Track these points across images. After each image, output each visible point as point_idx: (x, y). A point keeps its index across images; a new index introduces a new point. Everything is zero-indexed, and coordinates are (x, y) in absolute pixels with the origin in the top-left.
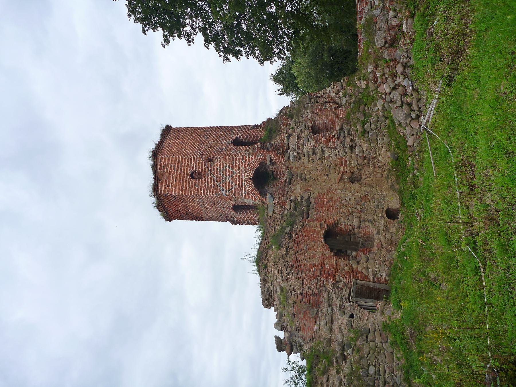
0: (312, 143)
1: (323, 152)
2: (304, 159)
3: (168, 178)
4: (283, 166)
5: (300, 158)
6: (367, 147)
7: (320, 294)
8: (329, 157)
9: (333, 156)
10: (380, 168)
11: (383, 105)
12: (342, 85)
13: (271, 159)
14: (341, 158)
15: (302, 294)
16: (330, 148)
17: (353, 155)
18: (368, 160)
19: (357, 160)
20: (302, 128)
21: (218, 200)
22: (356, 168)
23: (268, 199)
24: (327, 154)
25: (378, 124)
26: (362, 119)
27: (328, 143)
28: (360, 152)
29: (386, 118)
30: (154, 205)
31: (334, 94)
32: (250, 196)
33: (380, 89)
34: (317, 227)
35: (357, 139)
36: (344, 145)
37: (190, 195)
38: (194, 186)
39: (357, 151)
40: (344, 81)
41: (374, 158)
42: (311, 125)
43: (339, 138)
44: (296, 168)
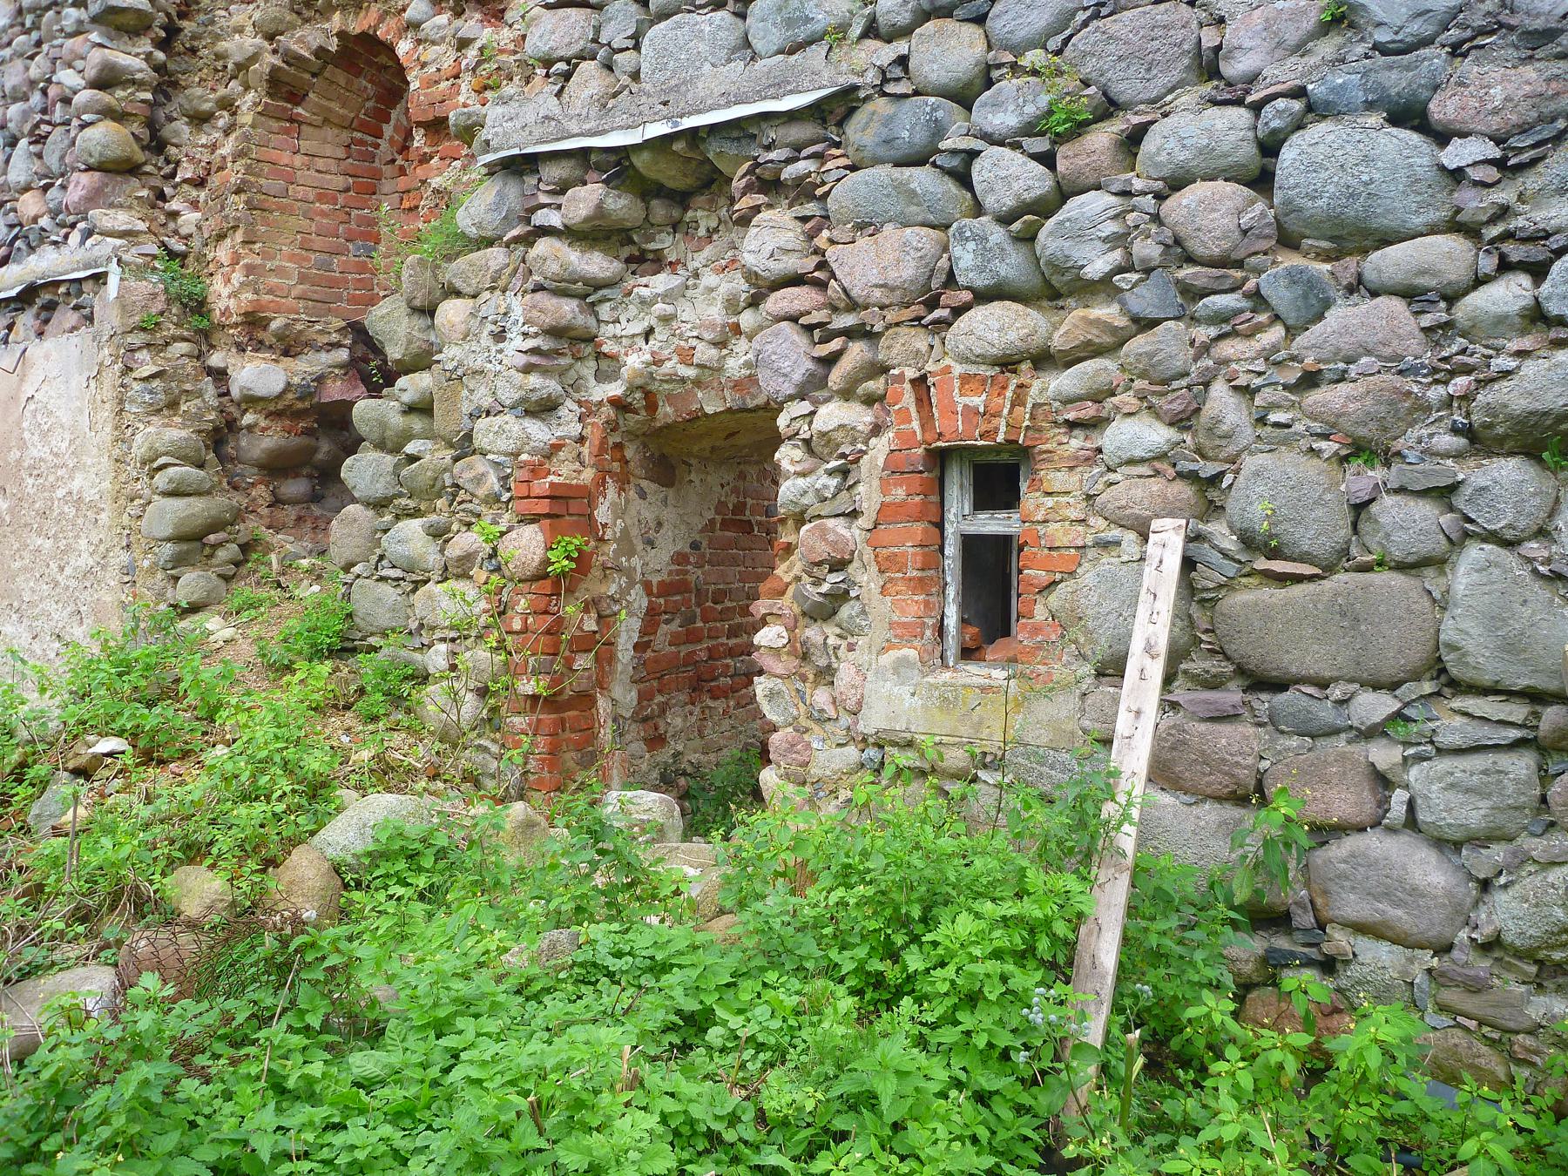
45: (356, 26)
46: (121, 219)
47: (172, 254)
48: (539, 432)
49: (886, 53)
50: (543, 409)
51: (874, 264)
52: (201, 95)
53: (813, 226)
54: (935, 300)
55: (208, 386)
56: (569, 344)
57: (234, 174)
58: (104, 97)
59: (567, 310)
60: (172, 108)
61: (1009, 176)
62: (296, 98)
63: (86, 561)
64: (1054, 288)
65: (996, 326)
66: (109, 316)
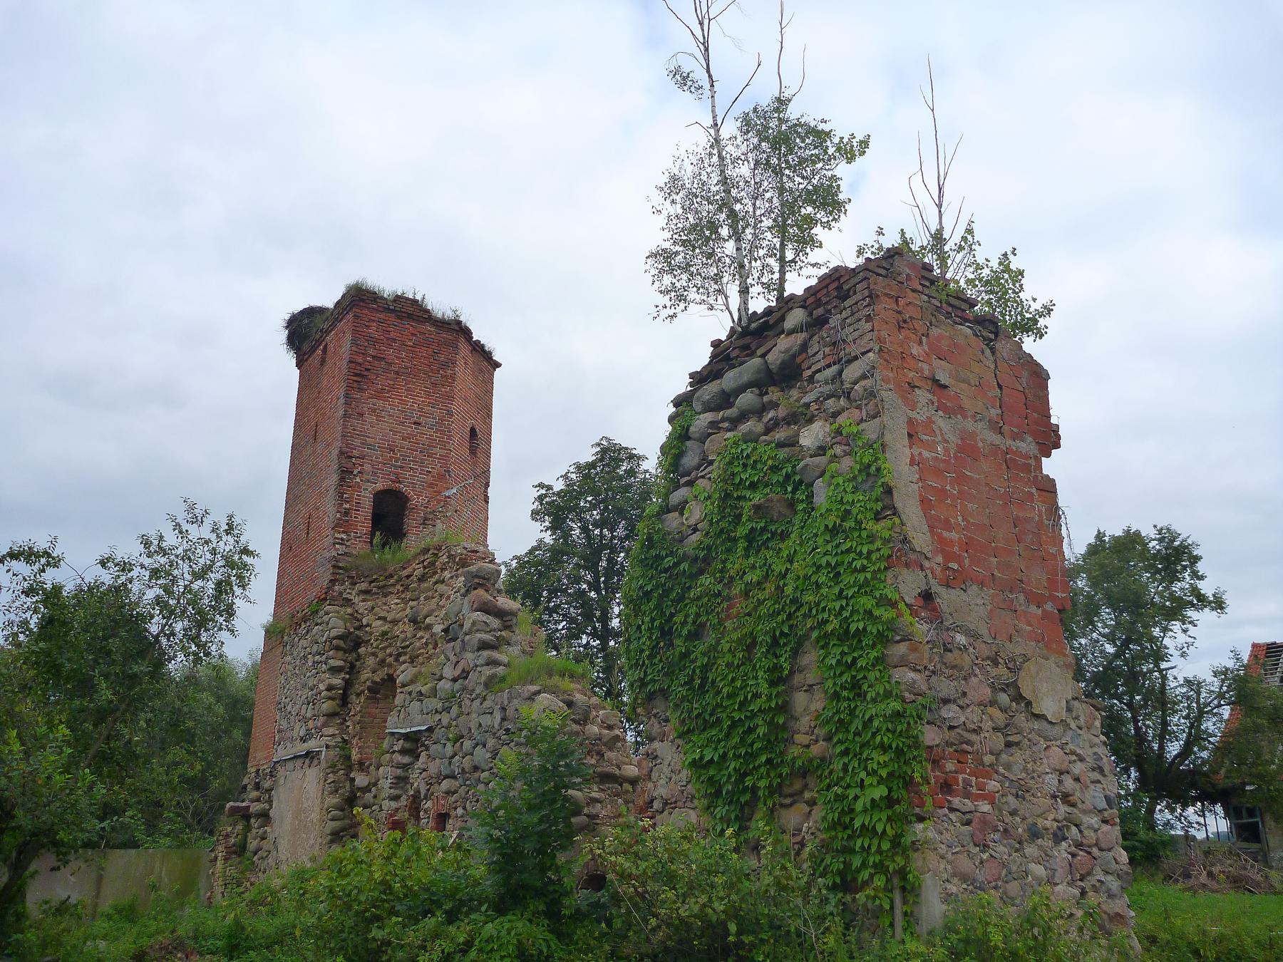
30: (419, 297)
45: (391, 672)
46: (331, 731)
47: (344, 741)
48: (394, 804)
49: (438, 717)
50: (396, 798)
51: (433, 768)
52: (358, 688)
53: (429, 756)
54: (441, 778)
55: (348, 784)
56: (401, 781)
57: (358, 718)
58: (329, 694)
59: (399, 771)
60: (352, 690)
61: (449, 749)
62: (377, 692)
63: (312, 842)
64: (454, 777)
65: (446, 785)
66: (324, 764)
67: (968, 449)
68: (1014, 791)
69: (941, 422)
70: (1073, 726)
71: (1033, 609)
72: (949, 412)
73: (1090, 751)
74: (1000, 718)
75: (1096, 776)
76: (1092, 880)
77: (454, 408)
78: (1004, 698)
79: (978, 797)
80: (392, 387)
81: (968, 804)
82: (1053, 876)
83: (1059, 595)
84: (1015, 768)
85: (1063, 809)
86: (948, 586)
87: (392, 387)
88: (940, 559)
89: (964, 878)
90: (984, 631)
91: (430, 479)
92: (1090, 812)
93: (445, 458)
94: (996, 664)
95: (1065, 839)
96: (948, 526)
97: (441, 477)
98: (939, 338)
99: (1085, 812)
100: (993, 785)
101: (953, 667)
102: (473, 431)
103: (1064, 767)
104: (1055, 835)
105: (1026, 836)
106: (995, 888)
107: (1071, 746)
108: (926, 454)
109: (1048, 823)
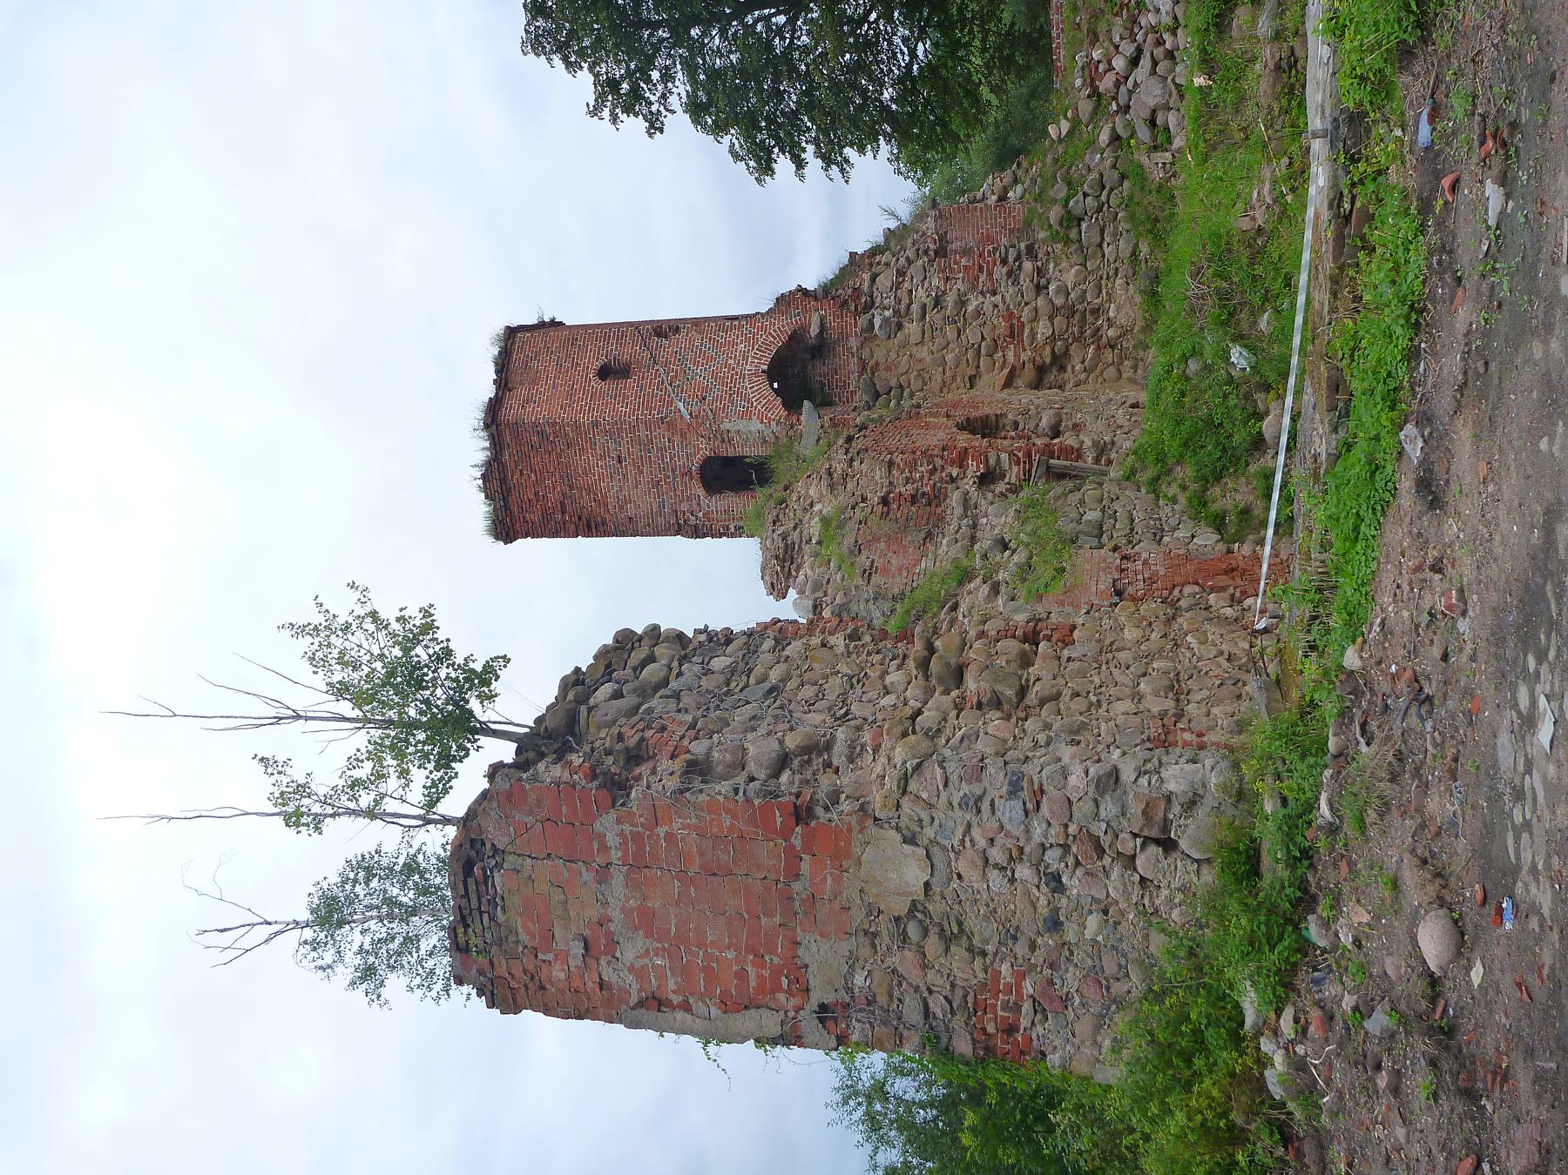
0: (935, 282)
1: (961, 303)
2: (912, 328)
3: (534, 383)
4: (854, 364)
5: (900, 326)
6: (1078, 273)
7: (936, 498)
8: (978, 313)
9: (987, 308)
10: (1113, 347)
11: (1113, 129)
12: (1014, 173)
13: (822, 326)
14: (1011, 315)
15: (885, 501)
16: (982, 293)
17: (1041, 301)
18: (1080, 318)
19: (1051, 319)
20: (910, 253)
21: (661, 435)
22: (1048, 349)
23: (802, 418)
24: (970, 308)
25: (1103, 198)
26: (1063, 194)
27: (977, 279)
28: (1058, 292)
29: (1123, 177)
31: (995, 198)
32: (754, 421)
33: (1107, 83)
34: (936, 415)
35: (1051, 266)
36: (1016, 282)
37: (586, 419)
38: (603, 395)
39: (1052, 288)
40: (1019, 165)
41: (1096, 312)
42: (932, 246)
43: (1004, 262)
44: (888, 369)
67: (645, 921)
68: (1010, 942)
69: (631, 951)
70: (930, 832)
71: (805, 866)
72: (613, 944)
73: (958, 812)
74: (933, 945)
75: (985, 806)
76: (1106, 841)
77: (586, 419)
78: (913, 930)
79: (1020, 995)
80: (589, 491)
81: (1027, 1007)
82: (1098, 901)
83: (779, 820)
84: (987, 934)
85: (1024, 872)
86: (808, 990)
87: (589, 491)
88: (782, 997)
89: (1098, 1028)
90: (845, 946)
91: (677, 439)
92: (1027, 831)
93: (648, 425)
94: (875, 935)
95: (1057, 877)
96: (742, 975)
97: (671, 426)
98: (532, 936)
99: (1029, 839)
100: (1005, 969)
101: (891, 996)
102: (604, 373)
103: (980, 862)
104: (1054, 891)
105: (1056, 937)
106: (1108, 988)
107: (956, 843)
108: (671, 985)
109: (1043, 901)
